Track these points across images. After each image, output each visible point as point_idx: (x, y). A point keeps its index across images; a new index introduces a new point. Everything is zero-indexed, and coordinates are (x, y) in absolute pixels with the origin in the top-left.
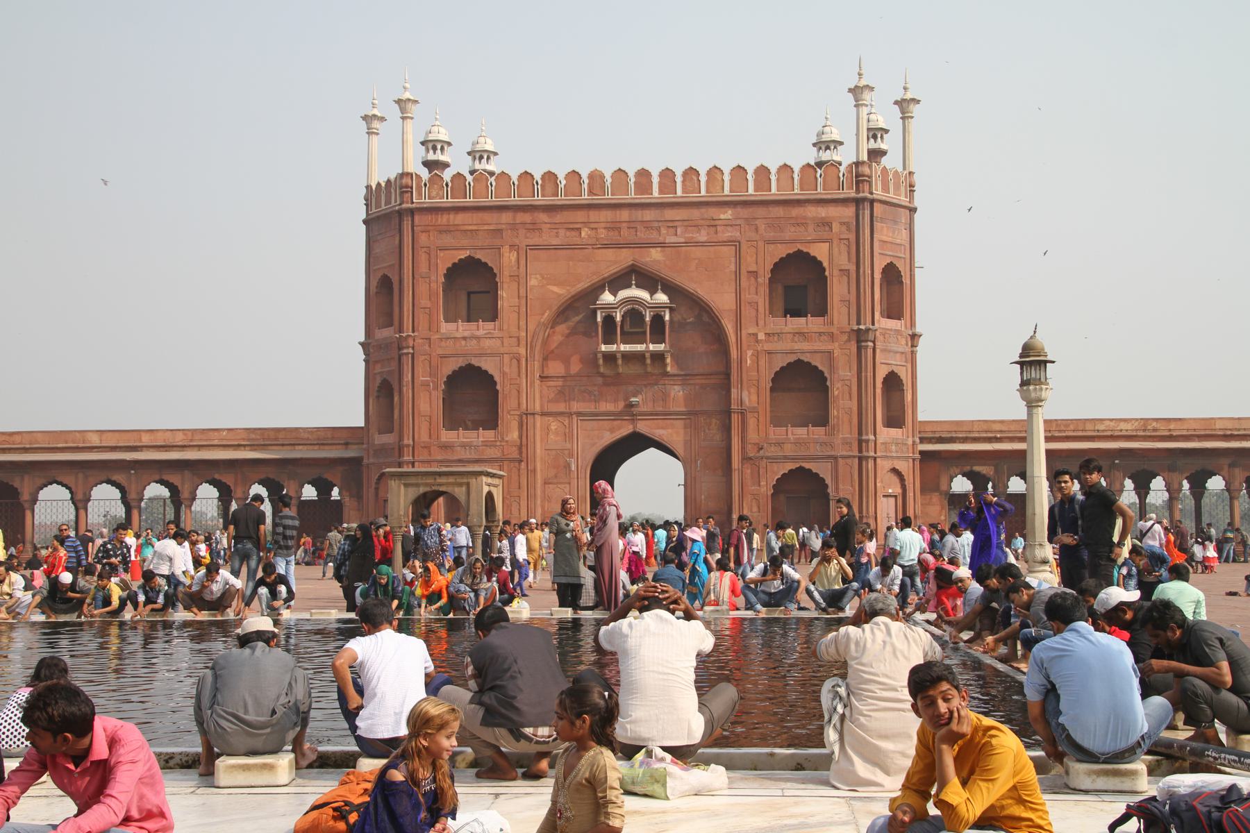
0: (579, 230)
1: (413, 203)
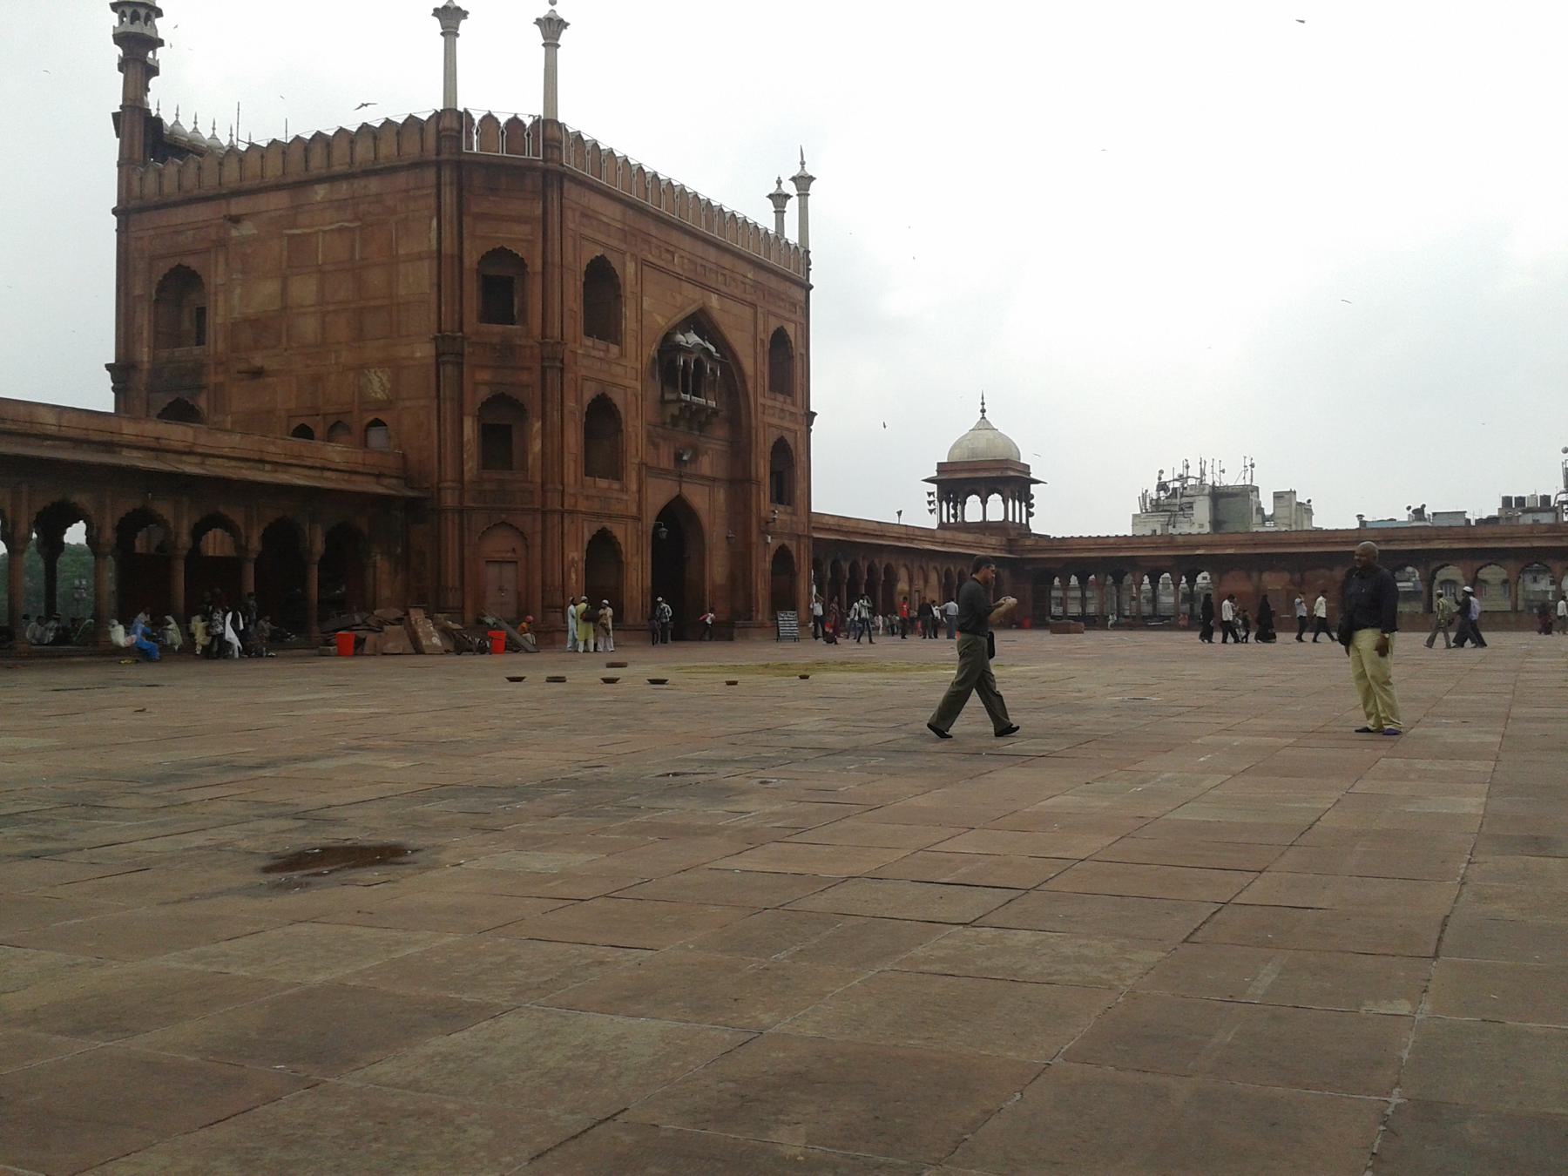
0: (673, 254)
1: (562, 165)
